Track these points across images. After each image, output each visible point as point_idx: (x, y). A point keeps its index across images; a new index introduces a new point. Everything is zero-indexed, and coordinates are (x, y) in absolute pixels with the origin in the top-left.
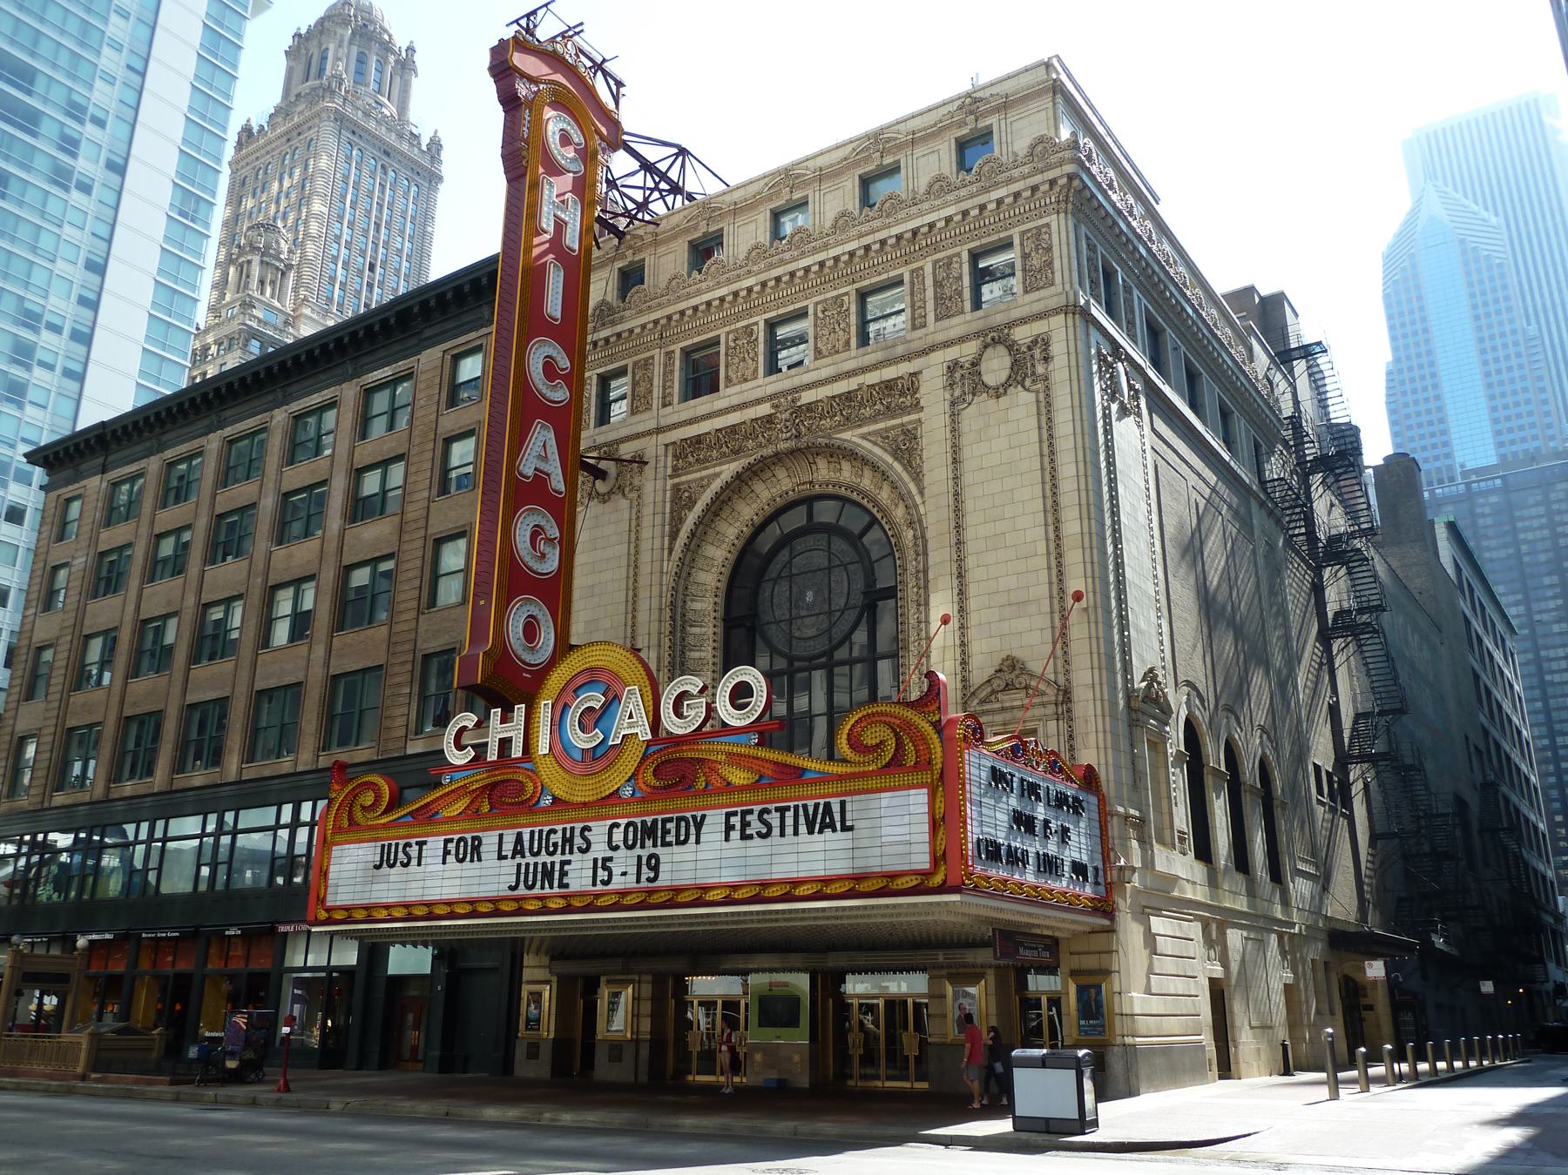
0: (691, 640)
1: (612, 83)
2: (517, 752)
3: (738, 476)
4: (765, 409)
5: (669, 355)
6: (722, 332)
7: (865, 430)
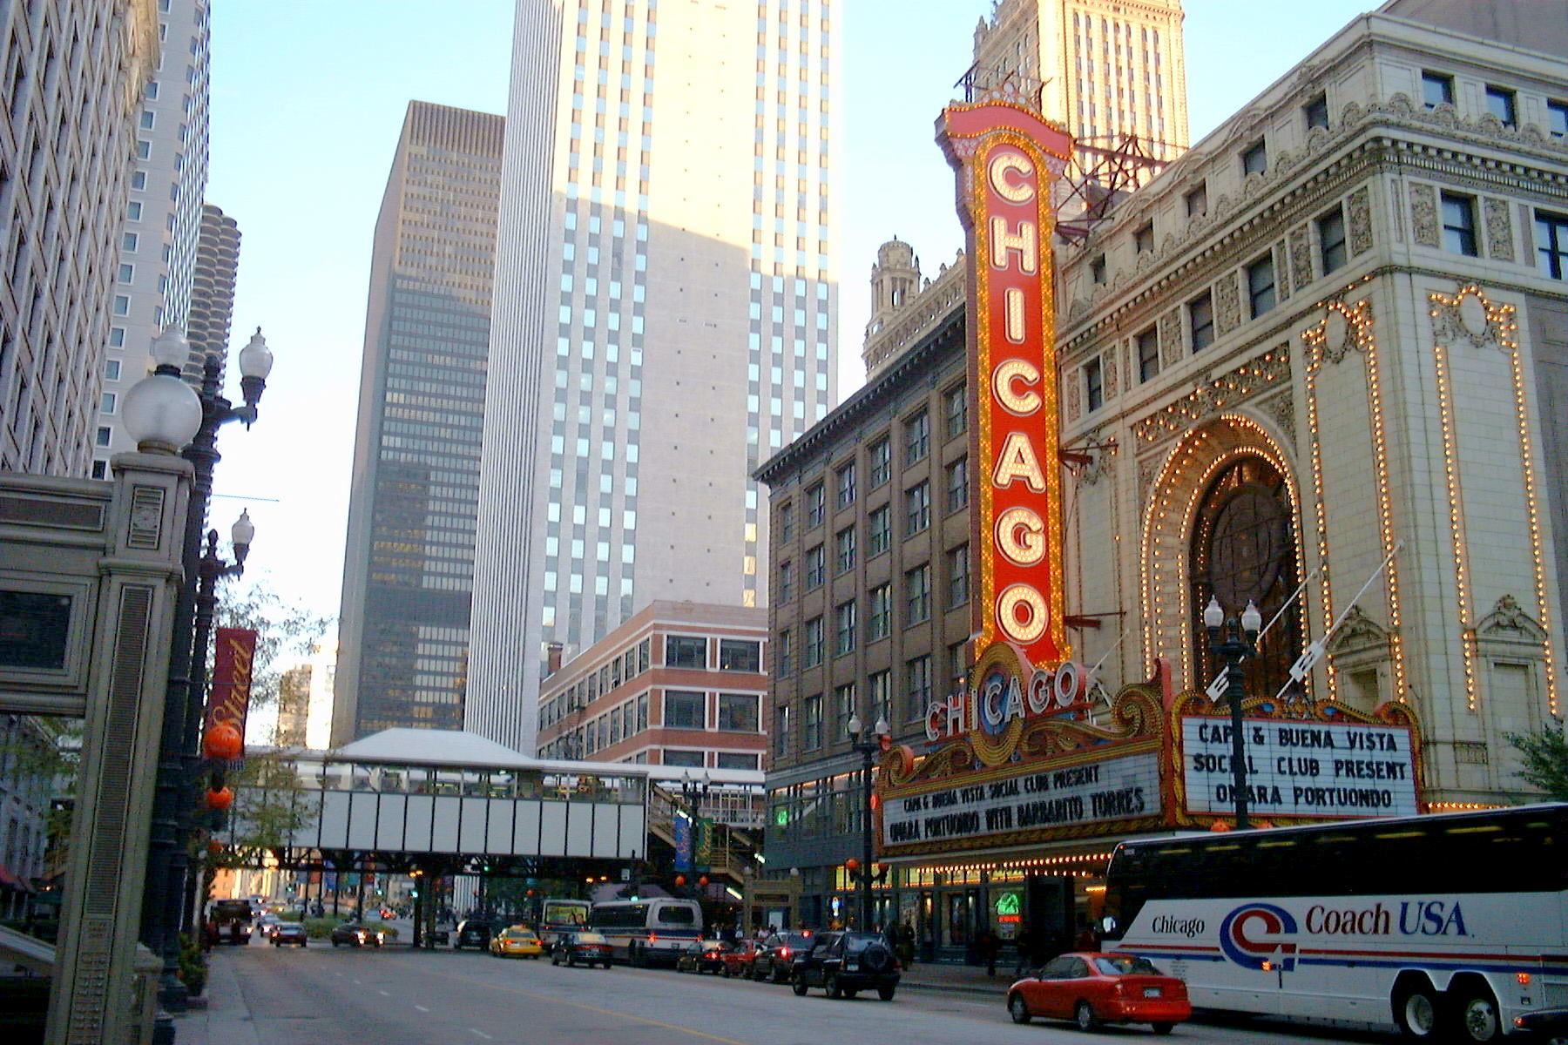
2: (961, 729)
4: (1189, 388)
6: (1157, 318)
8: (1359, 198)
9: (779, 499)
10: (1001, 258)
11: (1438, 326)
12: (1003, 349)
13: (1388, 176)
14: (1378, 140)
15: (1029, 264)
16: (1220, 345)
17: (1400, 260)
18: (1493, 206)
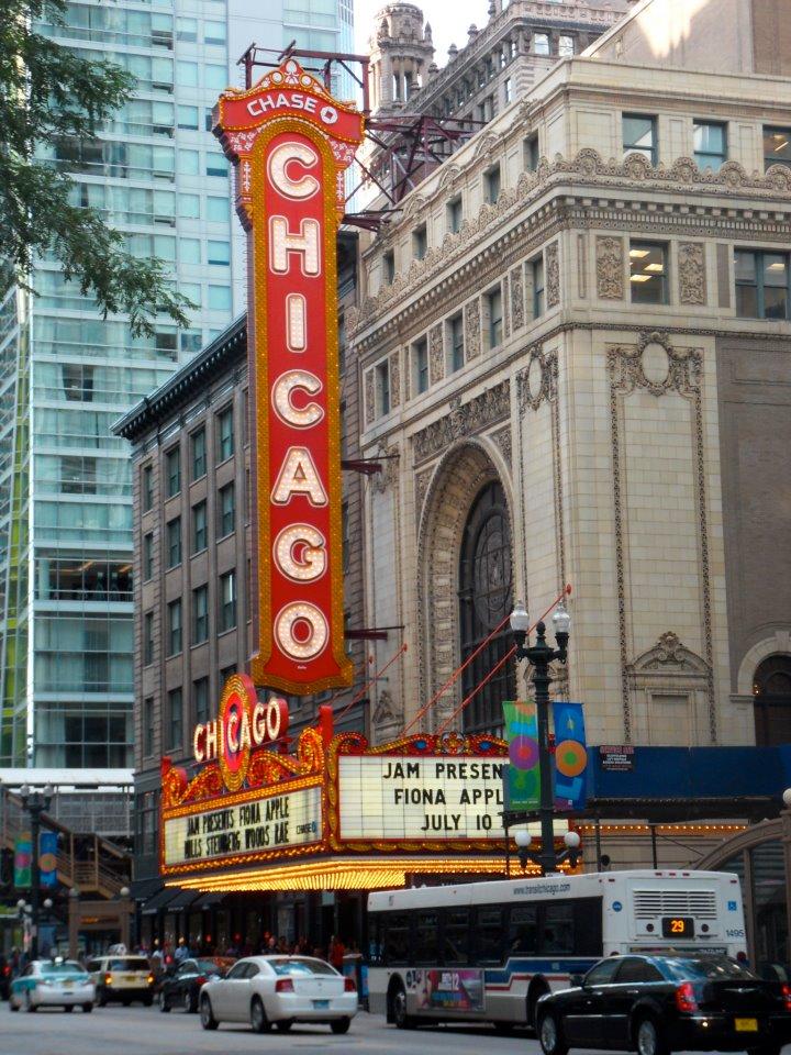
0: (439, 614)
1: (357, 68)
3: (442, 469)
4: (445, 410)
5: (407, 348)
7: (492, 430)
8: (552, 251)
9: (141, 459)
10: (280, 263)
11: (618, 378)
12: (282, 360)
13: (575, 232)
14: (561, 198)
15: (312, 265)
16: (472, 369)
17: (579, 318)
18: (689, 249)
